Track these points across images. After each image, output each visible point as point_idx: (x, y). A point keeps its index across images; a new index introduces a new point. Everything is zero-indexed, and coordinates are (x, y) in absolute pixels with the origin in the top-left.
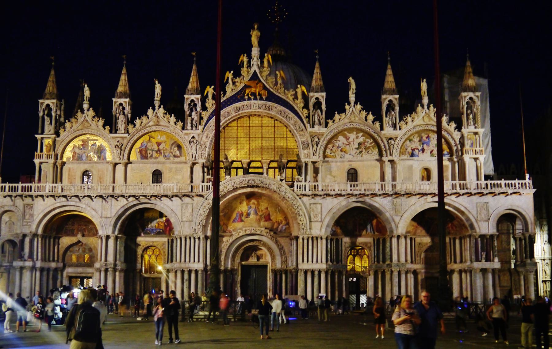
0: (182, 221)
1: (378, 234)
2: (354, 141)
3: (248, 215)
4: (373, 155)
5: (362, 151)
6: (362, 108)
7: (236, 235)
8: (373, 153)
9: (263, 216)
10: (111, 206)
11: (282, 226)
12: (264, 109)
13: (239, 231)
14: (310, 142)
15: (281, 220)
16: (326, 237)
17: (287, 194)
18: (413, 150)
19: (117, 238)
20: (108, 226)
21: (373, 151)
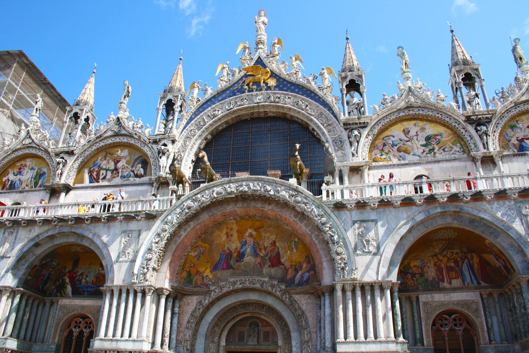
1: (486, 285)
2: (417, 135)
3: (241, 256)
4: (453, 154)
5: (433, 149)
7: (217, 291)
8: (453, 150)
9: (267, 258)
10: (15, 239)
11: (303, 274)
13: (222, 283)
15: (300, 262)
21: (452, 148)
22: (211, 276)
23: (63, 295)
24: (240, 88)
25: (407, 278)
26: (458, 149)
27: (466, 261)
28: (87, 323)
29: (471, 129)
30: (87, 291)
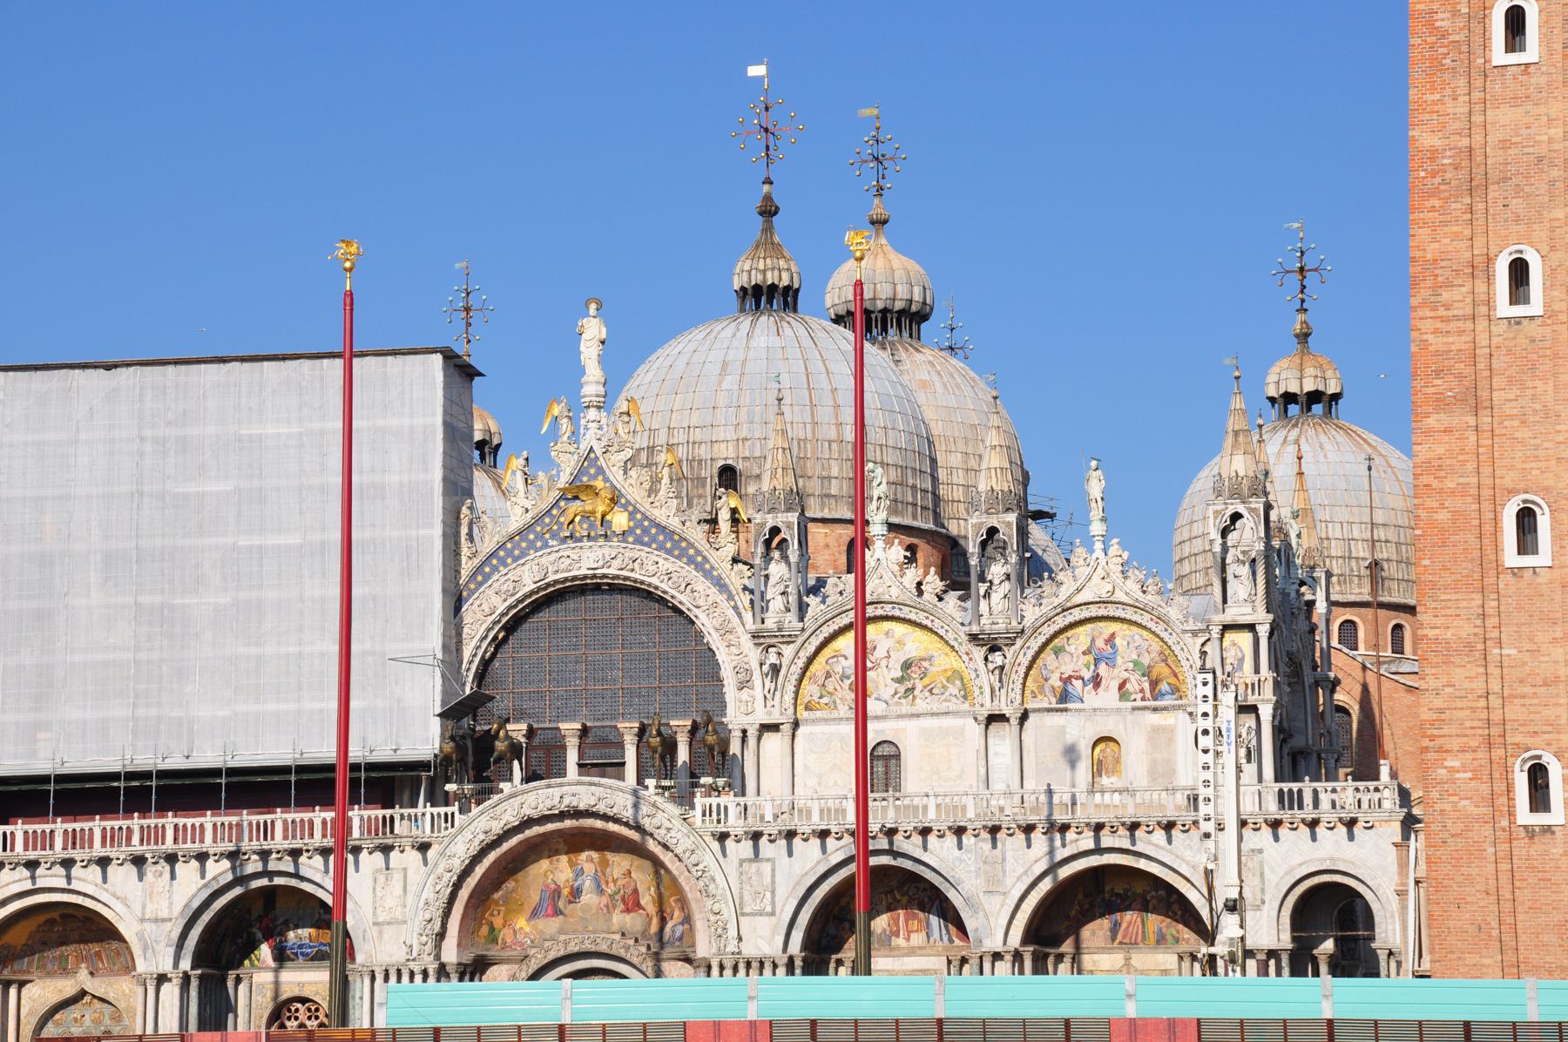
0: (374, 924)
3: (576, 893)
4: (946, 700)
5: (914, 689)
6: (906, 557)
7: (539, 956)
8: (947, 693)
9: (618, 897)
12: (622, 569)
13: (547, 944)
14: (755, 665)
16: (785, 960)
17: (673, 833)
18: (1067, 681)
19: (186, 978)
20: (163, 944)
22: (527, 929)
23: (256, 962)
24: (555, 527)
25: (843, 929)
26: (956, 692)
27: (937, 903)
28: (309, 1010)
29: (978, 653)
30: (302, 954)
